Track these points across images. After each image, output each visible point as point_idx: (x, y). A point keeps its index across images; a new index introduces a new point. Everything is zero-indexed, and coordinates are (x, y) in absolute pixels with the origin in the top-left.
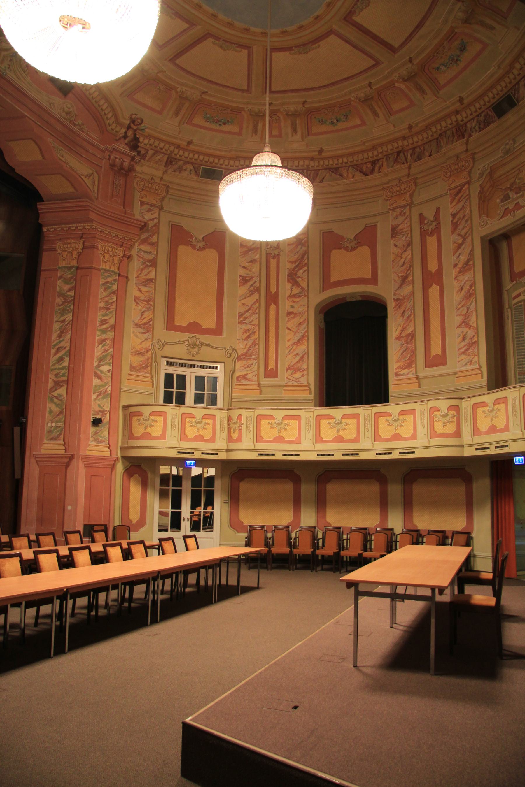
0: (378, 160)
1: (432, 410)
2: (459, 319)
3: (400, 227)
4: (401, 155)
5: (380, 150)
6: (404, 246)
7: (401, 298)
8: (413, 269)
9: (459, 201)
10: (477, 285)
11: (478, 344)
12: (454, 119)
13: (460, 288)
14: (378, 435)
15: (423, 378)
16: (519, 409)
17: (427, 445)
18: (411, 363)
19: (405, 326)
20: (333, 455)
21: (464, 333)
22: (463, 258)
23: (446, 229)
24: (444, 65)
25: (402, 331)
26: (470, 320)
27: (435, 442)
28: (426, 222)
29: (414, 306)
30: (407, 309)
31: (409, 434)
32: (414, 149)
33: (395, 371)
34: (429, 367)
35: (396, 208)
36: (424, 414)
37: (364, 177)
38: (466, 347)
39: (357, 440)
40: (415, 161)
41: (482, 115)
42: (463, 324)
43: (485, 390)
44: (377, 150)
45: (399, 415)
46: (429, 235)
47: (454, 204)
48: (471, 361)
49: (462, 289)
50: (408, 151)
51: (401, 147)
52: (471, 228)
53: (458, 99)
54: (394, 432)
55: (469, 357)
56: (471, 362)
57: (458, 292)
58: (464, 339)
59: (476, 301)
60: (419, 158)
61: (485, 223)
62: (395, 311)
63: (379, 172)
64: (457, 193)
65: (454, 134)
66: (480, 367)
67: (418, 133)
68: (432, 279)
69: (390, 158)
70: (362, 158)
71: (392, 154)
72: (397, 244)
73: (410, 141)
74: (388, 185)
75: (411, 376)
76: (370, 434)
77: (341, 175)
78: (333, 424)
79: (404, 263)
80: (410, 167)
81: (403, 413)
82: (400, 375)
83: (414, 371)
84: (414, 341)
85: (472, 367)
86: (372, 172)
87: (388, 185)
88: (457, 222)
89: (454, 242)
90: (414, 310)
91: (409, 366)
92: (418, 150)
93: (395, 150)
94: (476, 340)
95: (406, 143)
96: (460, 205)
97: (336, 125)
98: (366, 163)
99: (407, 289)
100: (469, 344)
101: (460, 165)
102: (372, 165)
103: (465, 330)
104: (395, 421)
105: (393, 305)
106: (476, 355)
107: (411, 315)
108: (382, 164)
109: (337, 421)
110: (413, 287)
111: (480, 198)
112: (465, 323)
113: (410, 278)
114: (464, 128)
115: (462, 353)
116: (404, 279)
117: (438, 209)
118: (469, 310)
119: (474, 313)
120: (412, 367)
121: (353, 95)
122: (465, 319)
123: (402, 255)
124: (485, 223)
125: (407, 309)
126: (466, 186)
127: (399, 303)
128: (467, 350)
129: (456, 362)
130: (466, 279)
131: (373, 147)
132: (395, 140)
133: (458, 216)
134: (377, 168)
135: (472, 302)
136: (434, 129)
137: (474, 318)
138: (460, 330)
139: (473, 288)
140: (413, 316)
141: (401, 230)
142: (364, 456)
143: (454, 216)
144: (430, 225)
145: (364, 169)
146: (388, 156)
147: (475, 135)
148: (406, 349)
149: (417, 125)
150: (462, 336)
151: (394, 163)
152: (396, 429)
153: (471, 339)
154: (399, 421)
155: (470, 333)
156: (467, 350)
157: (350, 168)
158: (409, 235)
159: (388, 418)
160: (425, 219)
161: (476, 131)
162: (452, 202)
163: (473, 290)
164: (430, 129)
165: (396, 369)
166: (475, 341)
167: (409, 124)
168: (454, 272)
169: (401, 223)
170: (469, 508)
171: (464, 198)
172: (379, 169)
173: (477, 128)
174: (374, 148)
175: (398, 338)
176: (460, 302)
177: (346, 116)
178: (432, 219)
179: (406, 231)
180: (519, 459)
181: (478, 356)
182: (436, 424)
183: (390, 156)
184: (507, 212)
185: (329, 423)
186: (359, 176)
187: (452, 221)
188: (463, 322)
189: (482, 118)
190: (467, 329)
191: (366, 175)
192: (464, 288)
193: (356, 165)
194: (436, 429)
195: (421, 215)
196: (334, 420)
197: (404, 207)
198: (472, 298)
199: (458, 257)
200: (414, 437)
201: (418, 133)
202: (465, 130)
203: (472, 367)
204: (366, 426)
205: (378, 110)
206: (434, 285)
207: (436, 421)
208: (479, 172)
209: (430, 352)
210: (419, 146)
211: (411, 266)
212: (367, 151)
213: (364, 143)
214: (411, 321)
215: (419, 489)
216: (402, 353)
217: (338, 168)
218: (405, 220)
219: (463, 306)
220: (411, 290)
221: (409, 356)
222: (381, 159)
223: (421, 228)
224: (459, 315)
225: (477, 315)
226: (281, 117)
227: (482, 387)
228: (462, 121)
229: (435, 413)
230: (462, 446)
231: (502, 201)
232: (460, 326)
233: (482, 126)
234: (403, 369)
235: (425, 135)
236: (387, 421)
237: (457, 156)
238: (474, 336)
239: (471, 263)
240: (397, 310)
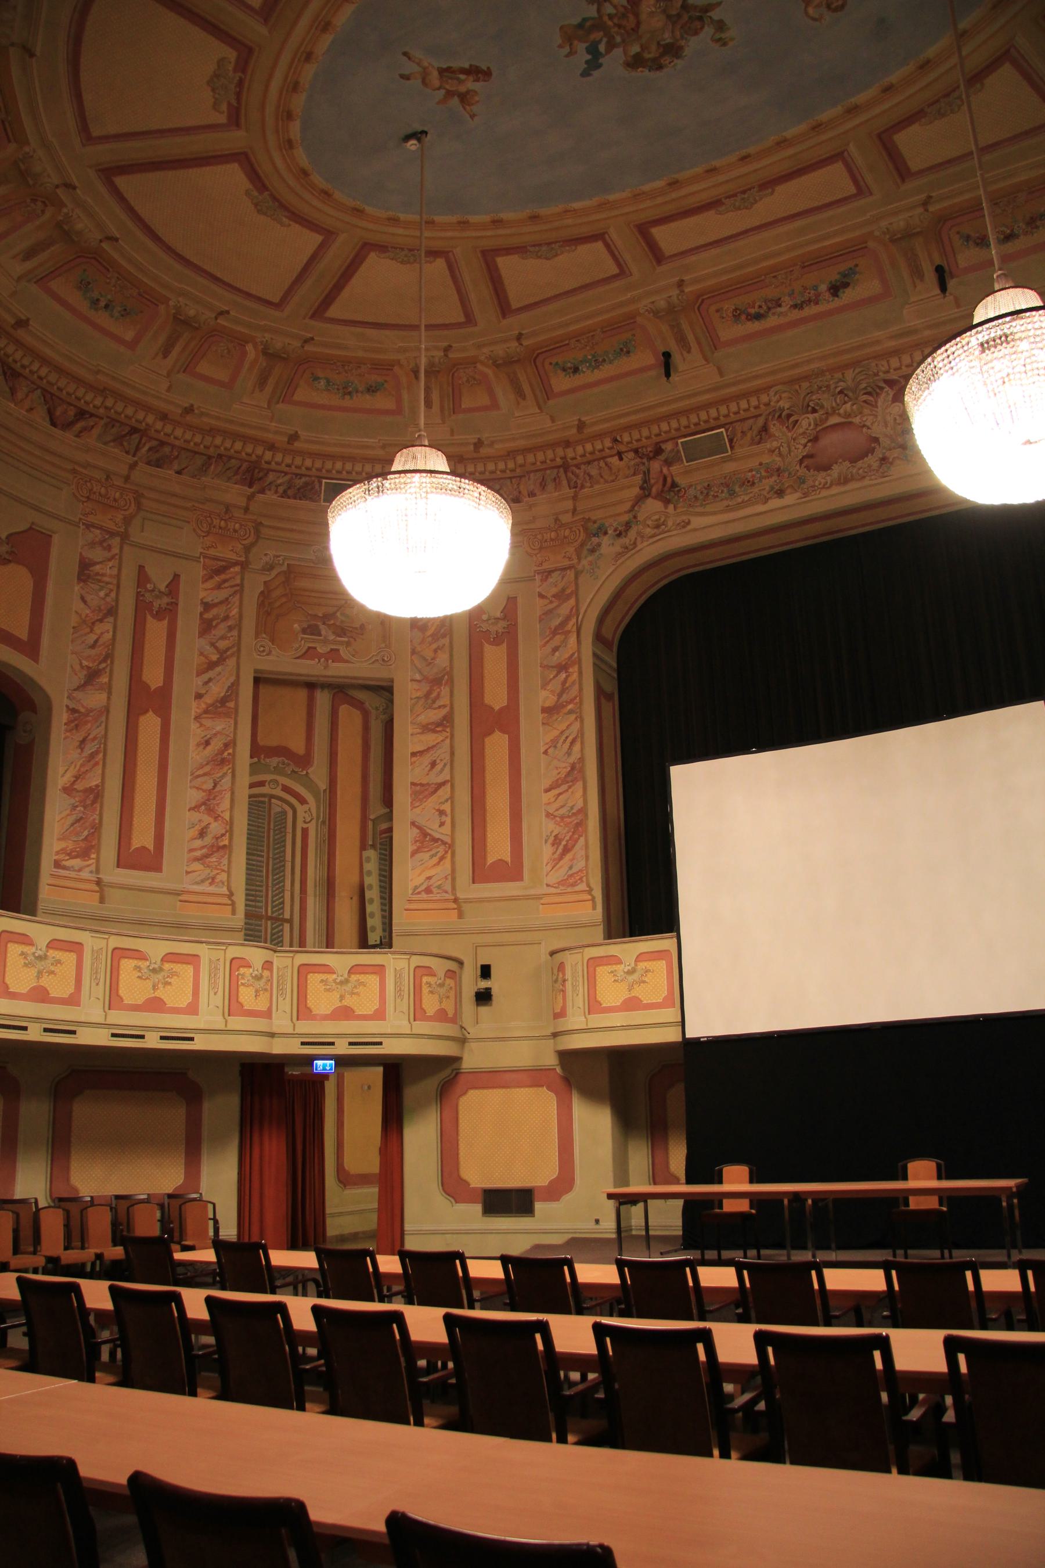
0: (92, 415)
1: (235, 964)
2: (195, 796)
3: (97, 568)
4: (136, 437)
5: (109, 403)
6: (100, 610)
7: (83, 710)
8: (112, 663)
9: (219, 587)
10: (239, 748)
11: (231, 852)
12: (259, 451)
13: (203, 741)
14: (118, 995)
15: (112, 886)
16: (406, 989)
17: (222, 1027)
18: (88, 849)
19: (83, 770)
20: (25, 1028)
21: (203, 825)
22: (217, 690)
23: (188, 621)
24: (328, 382)
25: (77, 778)
26: (218, 805)
27: (237, 1022)
28: (149, 586)
29: (106, 736)
30: (91, 737)
31: (184, 1001)
32: (162, 444)
33: (56, 857)
34: (126, 867)
35: (93, 526)
36: (216, 968)
37: (47, 424)
38: (205, 851)
39: (380, 1015)
40: (149, 463)
41: (303, 479)
42: (203, 807)
43: (240, 937)
44: (105, 398)
45: (162, 960)
46: (154, 617)
47: (210, 584)
48: (213, 879)
49: (207, 743)
50: (151, 438)
51: (147, 425)
52: (239, 644)
53: (292, 432)
54: (152, 994)
55: (208, 871)
56: (213, 881)
57: (198, 745)
58: (202, 834)
59: (233, 776)
60: (158, 464)
61: (267, 649)
62: (67, 731)
63: (78, 436)
64: (218, 570)
65: (240, 471)
66: (231, 894)
67: (190, 427)
68: (148, 699)
69: (113, 426)
70: (72, 391)
71: (122, 423)
72: (88, 598)
73: (168, 429)
74: (201, 506)
75: (85, 874)
76: (101, 991)
77: (13, 391)
78: (30, 958)
79: (96, 641)
80: (133, 466)
81: (171, 957)
82: (65, 868)
83: (93, 868)
84: (98, 805)
85: (212, 889)
86: (67, 426)
87: (201, 506)
88: (211, 620)
89: (201, 654)
90: (105, 744)
91: (84, 854)
92: (167, 450)
93: (133, 422)
94: (226, 842)
95: (159, 425)
96: (222, 594)
97: (96, 310)
98: (71, 405)
99: (94, 699)
100: (213, 846)
101: (231, 525)
102: (75, 416)
103: (207, 819)
104: (154, 971)
105: (65, 717)
106: (223, 871)
107: (97, 752)
108: (93, 427)
109: (39, 953)
110: (109, 698)
111: (261, 605)
112: (208, 805)
113: (104, 679)
114: (261, 474)
115: (197, 859)
116: (92, 676)
117: (176, 577)
118: (218, 788)
119: (228, 795)
120: (90, 859)
121: (180, 299)
122: (208, 800)
123: (93, 623)
124: (267, 649)
125: (91, 737)
126: (237, 569)
127: (76, 719)
128: (207, 856)
129: (179, 869)
130: (218, 728)
131: (211, 430)
132: (148, 409)
133: (214, 611)
134: (79, 425)
135: (225, 774)
136: (218, 441)
137: (226, 804)
138: (196, 816)
139: (230, 751)
140: (101, 755)
141: (97, 574)
142: (87, 1038)
143: (207, 606)
144: (157, 597)
145: (58, 412)
146: (113, 422)
147: (270, 496)
148: (81, 818)
149: (202, 414)
150: (198, 827)
151: (114, 441)
152: (38, 978)
153: (217, 838)
154: (162, 974)
155: (216, 828)
156: (207, 856)
157: (39, 391)
158: (113, 595)
159: (140, 963)
160: (148, 580)
161: (276, 492)
162: (206, 581)
163: (229, 754)
164: (214, 437)
165: (57, 853)
166: (225, 846)
167: (192, 406)
168: (196, 708)
169: (100, 563)
170: (193, 1150)
171: (232, 587)
172: (81, 432)
173: (281, 489)
174: (103, 391)
175: (68, 790)
176: (202, 767)
177: (125, 313)
178: (162, 587)
179: (107, 583)
180: (325, 1065)
181: (229, 873)
182: (242, 989)
183: (118, 424)
184: (309, 653)
185: (22, 954)
186: (40, 417)
187: (201, 614)
188: (204, 804)
189: (299, 482)
190: (211, 820)
191: (54, 424)
192: (213, 743)
193: (52, 395)
194: (241, 999)
195: (141, 568)
196: (33, 949)
197: (112, 534)
198: (226, 768)
199: (206, 683)
200: (192, 1009)
201: (190, 427)
202: (260, 479)
203: (212, 889)
204: (95, 972)
205: (178, 348)
206: (151, 713)
207: (243, 984)
208: (265, 559)
209: (130, 838)
210: (173, 446)
211: (109, 657)
212: (91, 387)
213: (98, 372)
214: (97, 764)
215: (85, 1111)
216: (72, 825)
217: (20, 375)
218: (110, 560)
219: (205, 774)
220: (104, 702)
221: (86, 833)
222: (97, 416)
223: (138, 593)
224: (197, 788)
225: (232, 800)
226: (48, 215)
227: (232, 930)
228: (266, 462)
229: (242, 970)
230: (272, 1035)
231: (304, 631)
232: (195, 808)
233: (290, 492)
234: (71, 855)
235: (198, 438)
236: (138, 968)
237: (228, 508)
238: (223, 835)
239: (231, 704)
240: (70, 731)
